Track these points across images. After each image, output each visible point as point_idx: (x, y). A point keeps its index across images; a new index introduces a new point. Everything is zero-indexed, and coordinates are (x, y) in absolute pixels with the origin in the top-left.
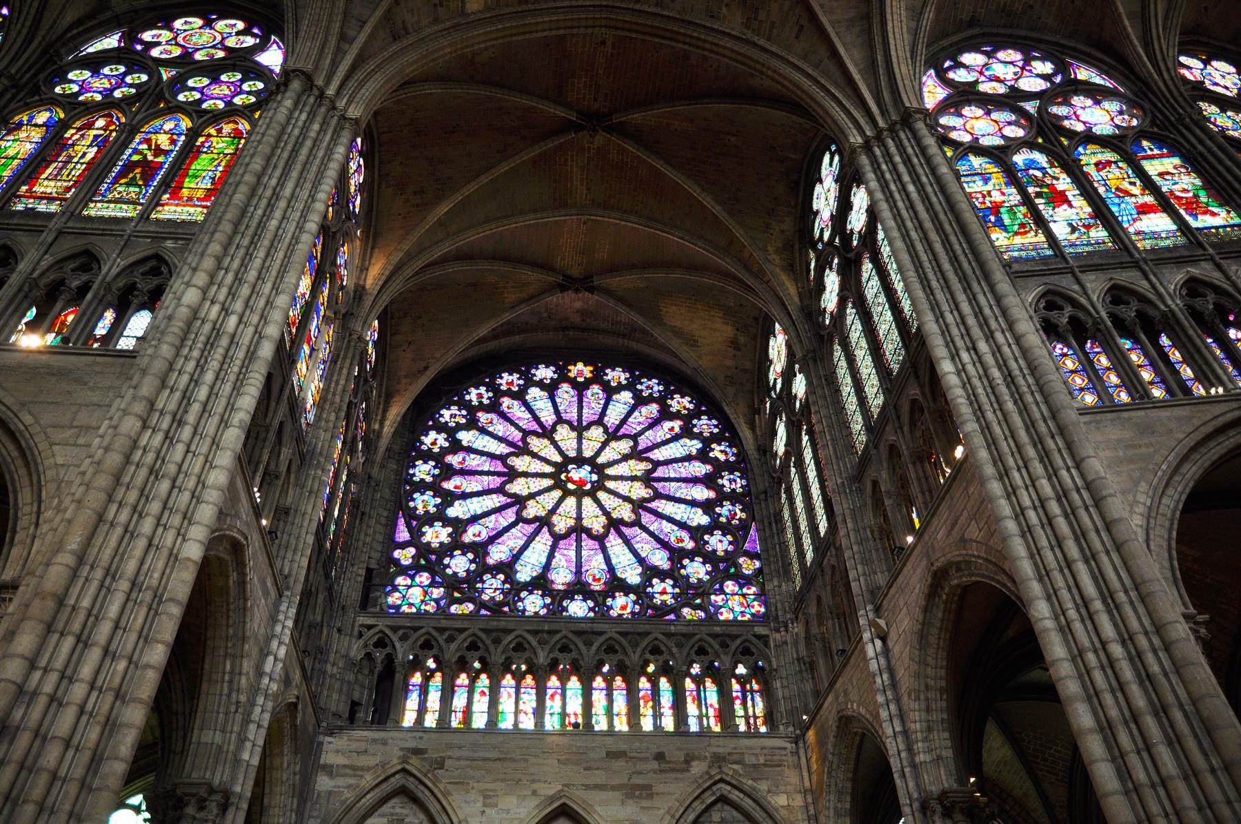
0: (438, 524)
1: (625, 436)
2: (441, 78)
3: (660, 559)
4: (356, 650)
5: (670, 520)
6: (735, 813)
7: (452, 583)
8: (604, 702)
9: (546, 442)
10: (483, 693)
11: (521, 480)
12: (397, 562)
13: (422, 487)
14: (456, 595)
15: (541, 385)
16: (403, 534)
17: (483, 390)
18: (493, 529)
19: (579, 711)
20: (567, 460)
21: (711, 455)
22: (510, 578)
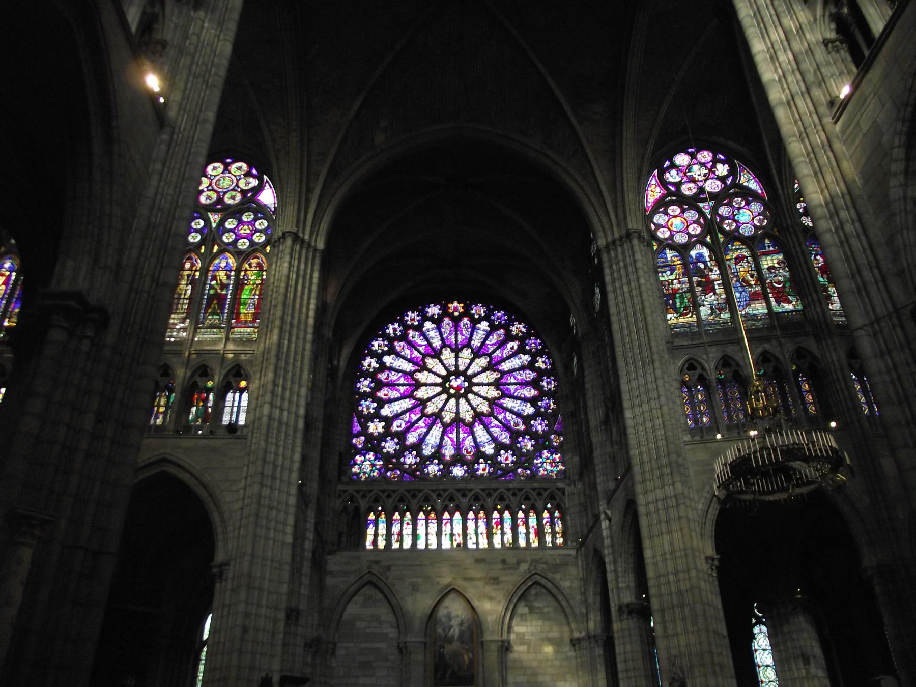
0: (376, 421)
1: (484, 355)
3: (505, 438)
5: (511, 411)
6: (544, 590)
7: (387, 458)
8: (474, 527)
10: (408, 524)
11: (423, 388)
12: (355, 446)
13: (365, 396)
15: (432, 319)
17: (396, 325)
18: (409, 422)
19: (461, 532)
21: (537, 365)
22: (419, 454)
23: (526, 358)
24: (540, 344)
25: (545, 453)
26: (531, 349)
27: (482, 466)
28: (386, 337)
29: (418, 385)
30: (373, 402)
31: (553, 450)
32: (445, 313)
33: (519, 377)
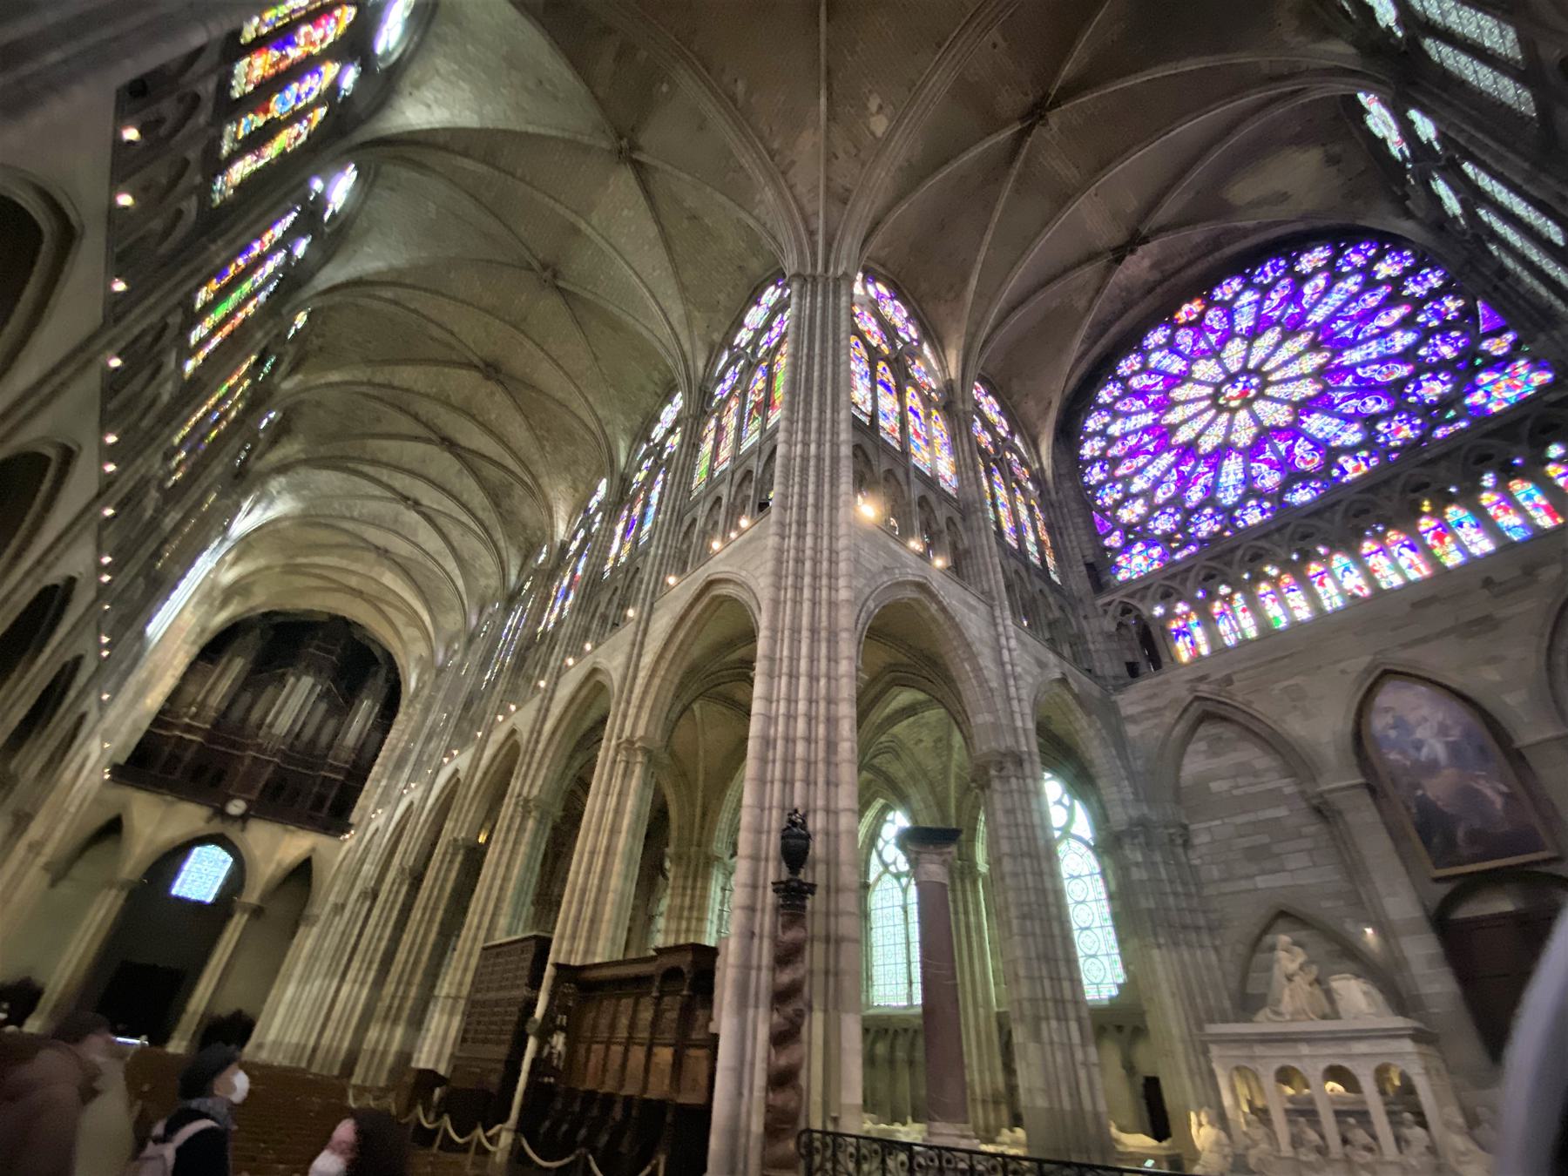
2: (899, 197)
4: (1110, 625)
7: (1167, 537)
11: (1183, 428)
12: (1110, 549)
17: (1110, 387)
20: (1218, 387)
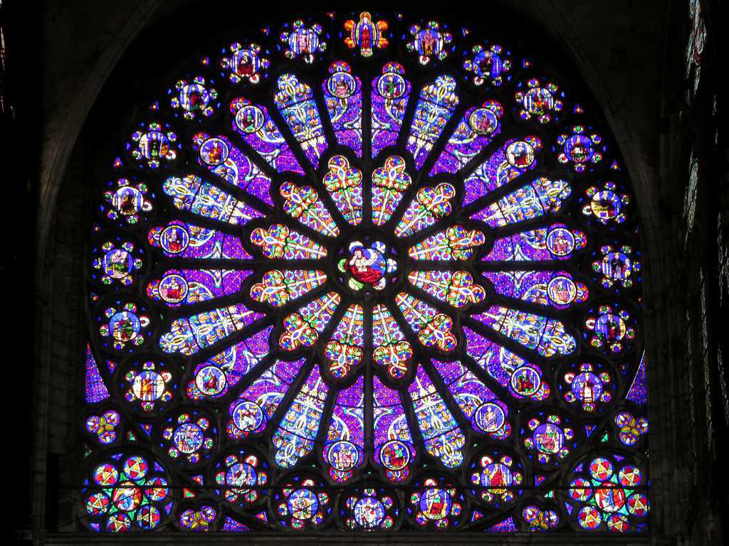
0: (149, 367)
1: (443, 177)
3: (493, 421)
5: (513, 346)
7: (179, 473)
9: (311, 194)
11: (275, 276)
12: (92, 439)
14: (188, 494)
16: (99, 390)
18: (235, 373)
22: (266, 464)
23: (558, 190)
24: (597, 149)
25: (600, 467)
26: (571, 164)
27: (433, 497)
28: (171, 119)
29: (260, 265)
30: (138, 313)
31: (620, 457)
32: (336, 49)
33: (535, 246)
